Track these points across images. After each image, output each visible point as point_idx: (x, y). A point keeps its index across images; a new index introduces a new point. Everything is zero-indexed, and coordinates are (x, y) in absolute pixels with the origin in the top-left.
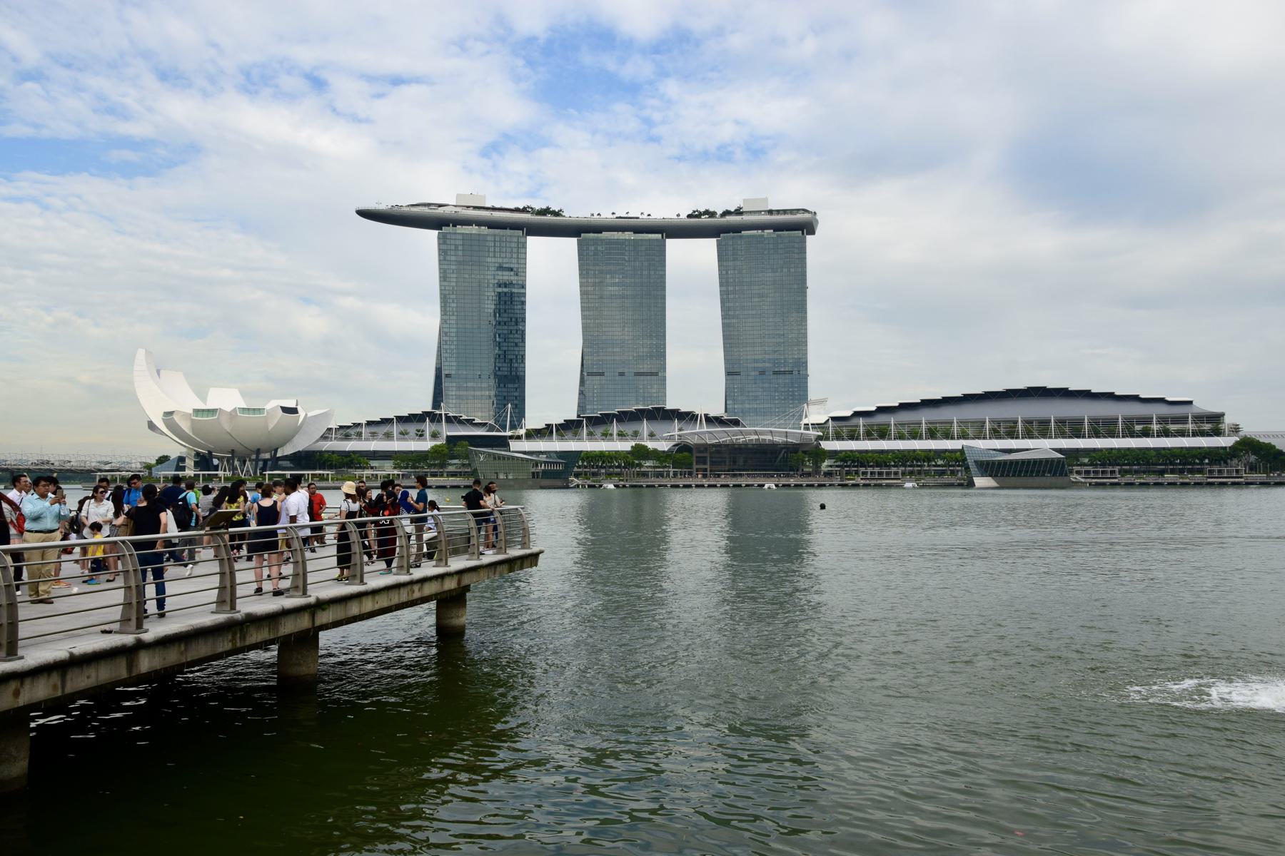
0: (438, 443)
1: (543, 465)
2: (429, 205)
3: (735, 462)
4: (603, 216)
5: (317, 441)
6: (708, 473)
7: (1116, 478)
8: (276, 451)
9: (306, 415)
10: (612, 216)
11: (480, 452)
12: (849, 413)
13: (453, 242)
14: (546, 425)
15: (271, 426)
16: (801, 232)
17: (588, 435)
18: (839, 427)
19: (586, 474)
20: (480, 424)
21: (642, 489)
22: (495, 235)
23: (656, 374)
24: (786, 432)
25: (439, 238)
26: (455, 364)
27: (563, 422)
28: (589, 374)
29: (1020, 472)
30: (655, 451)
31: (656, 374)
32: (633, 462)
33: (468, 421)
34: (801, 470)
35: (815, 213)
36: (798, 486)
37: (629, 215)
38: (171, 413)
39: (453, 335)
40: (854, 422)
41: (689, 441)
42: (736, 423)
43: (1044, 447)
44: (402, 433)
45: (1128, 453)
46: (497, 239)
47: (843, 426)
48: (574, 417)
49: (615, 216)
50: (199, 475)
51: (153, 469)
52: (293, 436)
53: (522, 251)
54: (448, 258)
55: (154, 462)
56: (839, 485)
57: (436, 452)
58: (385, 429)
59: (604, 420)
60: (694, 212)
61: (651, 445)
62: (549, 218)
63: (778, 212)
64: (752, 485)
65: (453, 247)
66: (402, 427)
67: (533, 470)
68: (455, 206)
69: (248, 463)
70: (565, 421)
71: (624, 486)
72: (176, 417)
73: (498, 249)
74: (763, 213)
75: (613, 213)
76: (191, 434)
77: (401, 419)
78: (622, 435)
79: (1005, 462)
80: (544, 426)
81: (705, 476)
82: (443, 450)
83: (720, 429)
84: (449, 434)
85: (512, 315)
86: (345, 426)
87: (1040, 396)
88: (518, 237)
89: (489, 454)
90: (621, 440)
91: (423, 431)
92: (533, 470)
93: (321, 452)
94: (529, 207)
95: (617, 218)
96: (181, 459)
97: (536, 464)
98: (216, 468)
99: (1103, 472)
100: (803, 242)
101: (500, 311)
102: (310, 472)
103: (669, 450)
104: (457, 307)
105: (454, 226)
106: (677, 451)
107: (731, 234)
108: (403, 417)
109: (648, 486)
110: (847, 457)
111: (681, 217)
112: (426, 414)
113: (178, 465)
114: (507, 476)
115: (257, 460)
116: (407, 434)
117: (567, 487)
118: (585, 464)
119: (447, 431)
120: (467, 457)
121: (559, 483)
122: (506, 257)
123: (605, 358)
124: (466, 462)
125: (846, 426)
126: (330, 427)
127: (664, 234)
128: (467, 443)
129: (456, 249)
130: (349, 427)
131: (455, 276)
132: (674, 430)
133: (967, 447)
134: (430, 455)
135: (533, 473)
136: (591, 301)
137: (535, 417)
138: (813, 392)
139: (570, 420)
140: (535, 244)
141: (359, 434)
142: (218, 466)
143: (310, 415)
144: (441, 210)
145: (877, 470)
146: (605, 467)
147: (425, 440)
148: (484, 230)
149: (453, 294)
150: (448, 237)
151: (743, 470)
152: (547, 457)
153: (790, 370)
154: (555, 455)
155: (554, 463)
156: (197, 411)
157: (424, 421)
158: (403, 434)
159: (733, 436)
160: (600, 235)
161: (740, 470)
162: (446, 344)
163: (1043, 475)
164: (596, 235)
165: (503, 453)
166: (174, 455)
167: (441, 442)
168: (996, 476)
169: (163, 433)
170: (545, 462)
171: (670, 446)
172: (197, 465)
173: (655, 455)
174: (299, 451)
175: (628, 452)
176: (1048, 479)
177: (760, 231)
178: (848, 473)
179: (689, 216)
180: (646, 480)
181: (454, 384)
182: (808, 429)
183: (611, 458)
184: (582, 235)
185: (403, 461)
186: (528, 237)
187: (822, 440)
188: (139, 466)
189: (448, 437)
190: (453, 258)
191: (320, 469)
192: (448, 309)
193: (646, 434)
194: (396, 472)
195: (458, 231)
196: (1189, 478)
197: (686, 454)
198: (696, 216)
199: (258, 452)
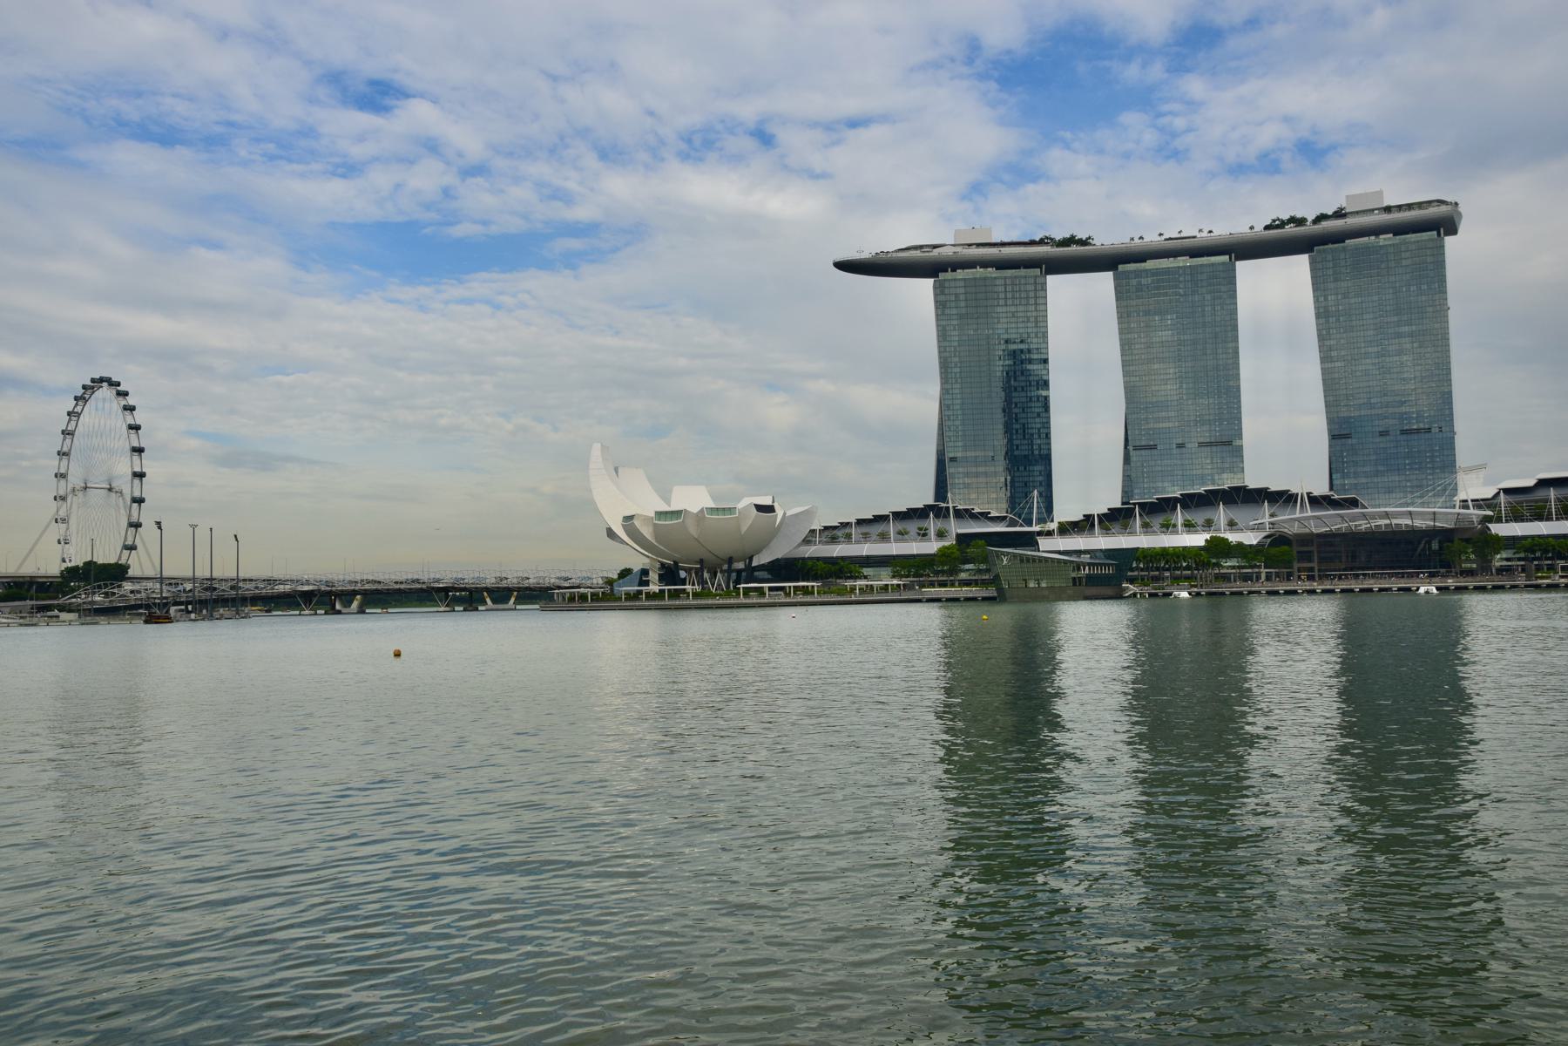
0: (947, 544)
3: (1354, 557)
5: (799, 545)
6: (1316, 573)
8: (751, 559)
9: (785, 514)
10: (1159, 238)
11: (1003, 553)
12: (1531, 482)
13: (952, 291)
15: (744, 529)
16: (1435, 233)
18: (1517, 503)
19: (1143, 579)
21: (1222, 598)
22: (1005, 278)
24: (1434, 513)
25: (935, 288)
28: (1136, 448)
30: (1240, 545)
31: (1229, 443)
32: (1209, 562)
33: (982, 514)
35: (1456, 204)
36: (1459, 589)
37: (1183, 235)
38: (631, 518)
39: (958, 407)
40: (1540, 494)
41: (1286, 530)
42: (1354, 503)
44: (900, 533)
47: (1524, 502)
48: (1119, 505)
49: (1163, 238)
50: (664, 590)
51: (615, 584)
52: (770, 542)
53: (1041, 294)
54: (948, 311)
55: (616, 577)
56: (1526, 586)
57: (943, 555)
58: (879, 528)
59: (1163, 507)
60: (1274, 221)
61: (1233, 537)
62: (1074, 248)
63: (1400, 207)
64: (1390, 589)
65: (953, 298)
66: (901, 526)
69: (719, 574)
70: (1109, 509)
72: (637, 522)
73: (1009, 295)
74: (1376, 212)
75: (1161, 235)
76: (653, 541)
77: (898, 516)
78: (1189, 526)
80: (1082, 518)
81: (1311, 578)
82: (952, 553)
84: (960, 531)
86: (831, 527)
88: (1036, 277)
89: (1015, 555)
90: (1189, 532)
91: (926, 529)
92: (1074, 575)
93: (803, 559)
94: (1047, 238)
95: (1166, 240)
96: (645, 572)
97: (1078, 567)
98: (683, 582)
100: (1440, 250)
101: (1015, 373)
102: (792, 584)
103: (1259, 544)
105: (954, 270)
106: (1270, 545)
107: (1330, 246)
108: (900, 512)
109: (1232, 593)
110: (1536, 545)
111: (1256, 230)
112: (928, 508)
113: (641, 579)
114: (1039, 584)
115: (730, 571)
116: (907, 533)
118: (1141, 566)
119: (956, 528)
120: (985, 560)
121: (1109, 591)
123: (1157, 426)
124: (983, 567)
125: (1527, 501)
126: (812, 528)
128: (982, 542)
130: (835, 528)
132: (1264, 517)
134: (936, 558)
135: (1074, 579)
136: (1135, 352)
137: (1067, 508)
140: (1057, 284)
141: (849, 536)
142: (685, 579)
143: (789, 513)
146: (1168, 570)
148: (991, 272)
150: (947, 284)
151: (1368, 569)
153: (1427, 426)
154: (1101, 555)
155: (1101, 565)
156: (660, 514)
157: (927, 516)
158: (902, 534)
160: (1143, 264)
161: (1359, 569)
162: (949, 420)
164: (1138, 265)
165: (1029, 553)
166: (636, 568)
167: (950, 542)
169: (623, 542)
170: (1089, 564)
171: (1260, 538)
172: (662, 578)
173: (1240, 550)
174: (777, 560)
175: (1200, 548)
177: (1373, 238)
178: (1539, 568)
179: (1267, 228)
180: (1228, 585)
181: (961, 470)
182: (1468, 508)
183: (1178, 557)
184: (1121, 267)
185: (903, 568)
187: (1491, 522)
188: (600, 581)
189: (959, 536)
190: (954, 311)
191: (803, 580)
193: (1223, 522)
194: (895, 582)
198: (1277, 227)
199: (730, 561)
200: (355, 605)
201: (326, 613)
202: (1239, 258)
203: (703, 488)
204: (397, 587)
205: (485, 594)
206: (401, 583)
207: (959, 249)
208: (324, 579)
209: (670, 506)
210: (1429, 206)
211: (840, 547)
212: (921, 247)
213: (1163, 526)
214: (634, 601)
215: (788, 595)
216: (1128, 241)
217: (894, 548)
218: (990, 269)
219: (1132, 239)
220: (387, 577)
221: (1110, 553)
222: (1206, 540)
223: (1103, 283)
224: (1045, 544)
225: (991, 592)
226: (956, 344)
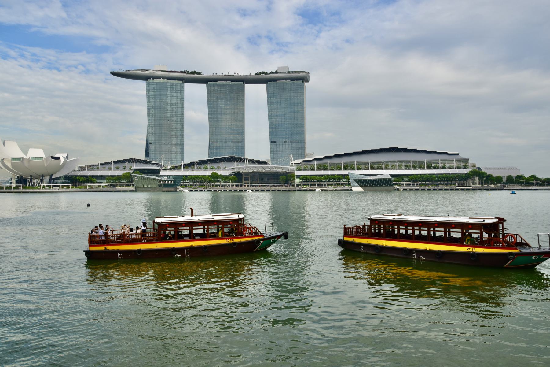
1: (163, 181)
2: (142, 70)
3: (262, 180)
6: (249, 185)
7: (418, 187)
10: (222, 75)
13: (152, 86)
20: (155, 164)
22: (170, 83)
23: (240, 142)
26: (153, 138)
27: (190, 163)
29: (373, 184)
31: (240, 142)
37: (229, 74)
43: (385, 174)
45: (424, 176)
46: (171, 84)
49: (223, 74)
54: (150, 93)
65: (152, 88)
67: (159, 184)
68: (154, 70)
73: (172, 89)
75: (222, 73)
79: (369, 180)
85: (178, 117)
87: (395, 151)
88: (181, 83)
99: (413, 184)
105: (153, 79)
107: (273, 82)
121: (172, 189)
122: (175, 92)
125: (309, 165)
129: (154, 89)
131: (153, 100)
133: (350, 173)
144: (147, 72)
148: (166, 80)
149: (152, 108)
150: (150, 83)
160: (216, 82)
161: (264, 183)
163: (382, 186)
168: (362, 186)
173: (221, 177)
175: (210, 176)
176: (385, 187)
177: (285, 81)
179: (255, 74)
181: (153, 147)
184: (209, 82)
190: (152, 93)
192: (150, 115)
196: (450, 187)
207: (155, 72)
212: (139, 70)
216: (212, 74)
218: (166, 80)
219: (213, 74)
222: (211, 174)
223: (203, 87)
226: (153, 104)
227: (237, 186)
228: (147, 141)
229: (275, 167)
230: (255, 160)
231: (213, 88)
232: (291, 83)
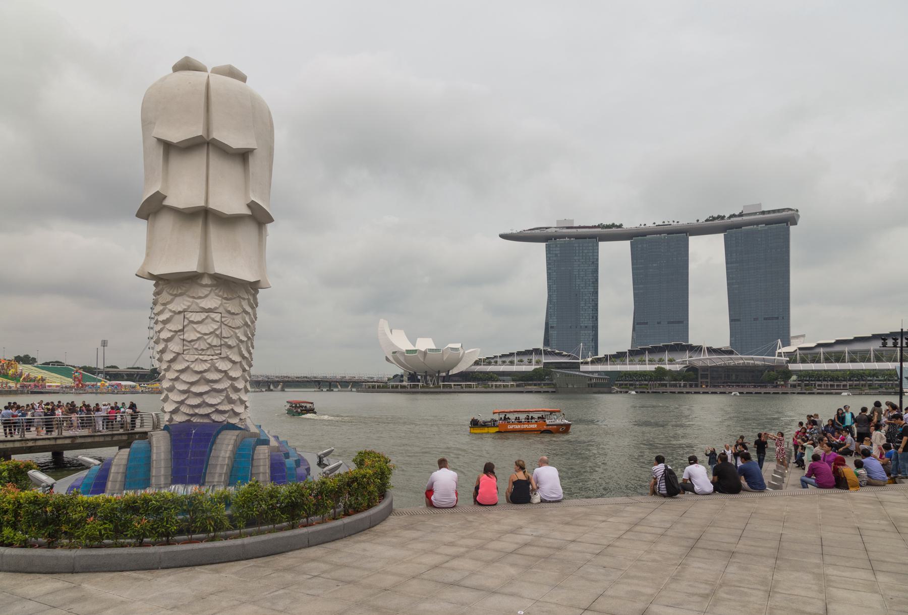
2: (541, 228)
4: (648, 225)
5: (471, 366)
8: (449, 371)
12: (813, 345)
14: (605, 355)
16: (785, 224)
17: (629, 361)
18: (803, 354)
20: (566, 355)
24: (764, 358)
27: (616, 353)
34: (775, 383)
42: (731, 352)
44: (519, 361)
47: (808, 354)
49: (655, 225)
55: (392, 377)
58: (510, 359)
59: (641, 352)
61: (667, 367)
62: (614, 229)
66: (519, 358)
68: (556, 228)
70: (617, 353)
71: (648, 392)
77: (519, 353)
78: (651, 362)
83: (715, 357)
90: (649, 364)
91: (531, 360)
92: (589, 382)
95: (657, 226)
96: (402, 376)
98: (419, 381)
103: (680, 371)
104: (557, 287)
105: (555, 239)
106: (687, 370)
107: (735, 230)
108: (522, 352)
109: (671, 392)
113: (400, 380)
117: (610, 393)
119: (545, 359)
125: (810, 354)
127: (688, 234)
138: (793, 332)
139: (620, 352)
140: (604, 247)
141: (496, 362)
143: (466, 352)
145: (830, 383)
147: (532, 365)
150: (551, 246)
152: (598, 375)
154: (603, 373)
159: (728, 361)
160: (645, 237)
165: (577, 373)
172: (409, 379)
174: (462, 372)
177: (755, 226)
179: (707, 220)
180: (665, 389)
181: (555, 332)
182: (781, 356)
184: (634, 238)
186: (600, 243)
188: (387, 379)
189: (544, 363)
195: (558, 242)
197: (691, 373)
198: (711, 220)
200: (280, 387)
201: (266, 390)
202: (691, 235)
203: (431, 339)
204: (297, 380)
205: (338, 384)
206: (299, 378)
208: (265, 374)
209: (414, 346)
210: (784, 211)
211: (491, 367)
213: (640, 361)
214: (395, 389)
215: (462, 388)
217: (514, 368)
218: (572, 239)
220: (293, 375)
221: (607, 373)
224: (583, 368)
225: (554, 390)
227: (691, 386)
228: (547, 324)
229: (752, 359)
230: (714, 348)
231: (640, 246)
232: (766, 228)
